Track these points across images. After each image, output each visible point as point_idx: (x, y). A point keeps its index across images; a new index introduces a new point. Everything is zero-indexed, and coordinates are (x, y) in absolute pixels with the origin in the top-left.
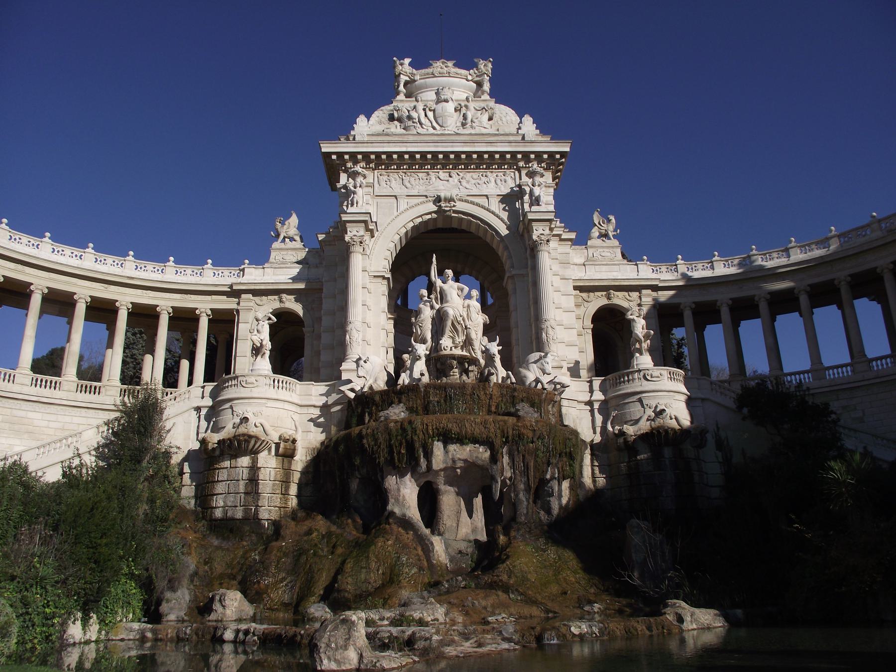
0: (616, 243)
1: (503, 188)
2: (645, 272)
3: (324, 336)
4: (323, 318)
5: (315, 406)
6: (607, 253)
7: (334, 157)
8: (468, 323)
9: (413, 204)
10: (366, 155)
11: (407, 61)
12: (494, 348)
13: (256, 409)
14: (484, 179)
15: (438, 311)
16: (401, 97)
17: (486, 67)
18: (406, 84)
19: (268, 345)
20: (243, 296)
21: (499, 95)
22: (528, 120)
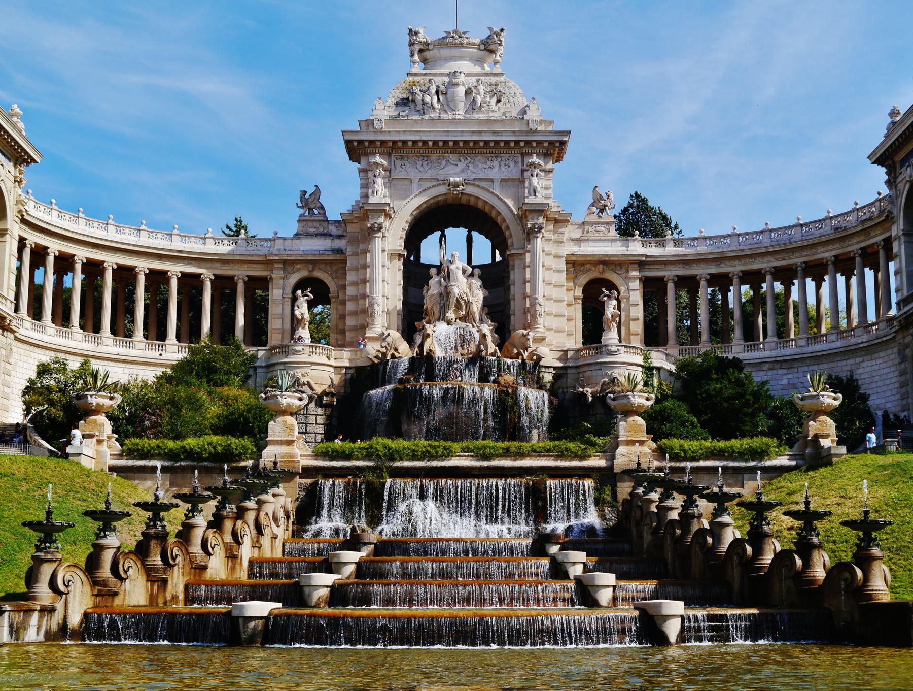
1: (506, 173)
3: (348, 303)
4: (348, 288)
7: (355, 144)
8: (471, 298)
9: (426, 187)
10: (383, 142)
12: (487, 329)
13: (304, 371)
14: (489, 163)
15: (446, 287)
18: (421, 51)
19: (307, 316)
20: (276, 265)
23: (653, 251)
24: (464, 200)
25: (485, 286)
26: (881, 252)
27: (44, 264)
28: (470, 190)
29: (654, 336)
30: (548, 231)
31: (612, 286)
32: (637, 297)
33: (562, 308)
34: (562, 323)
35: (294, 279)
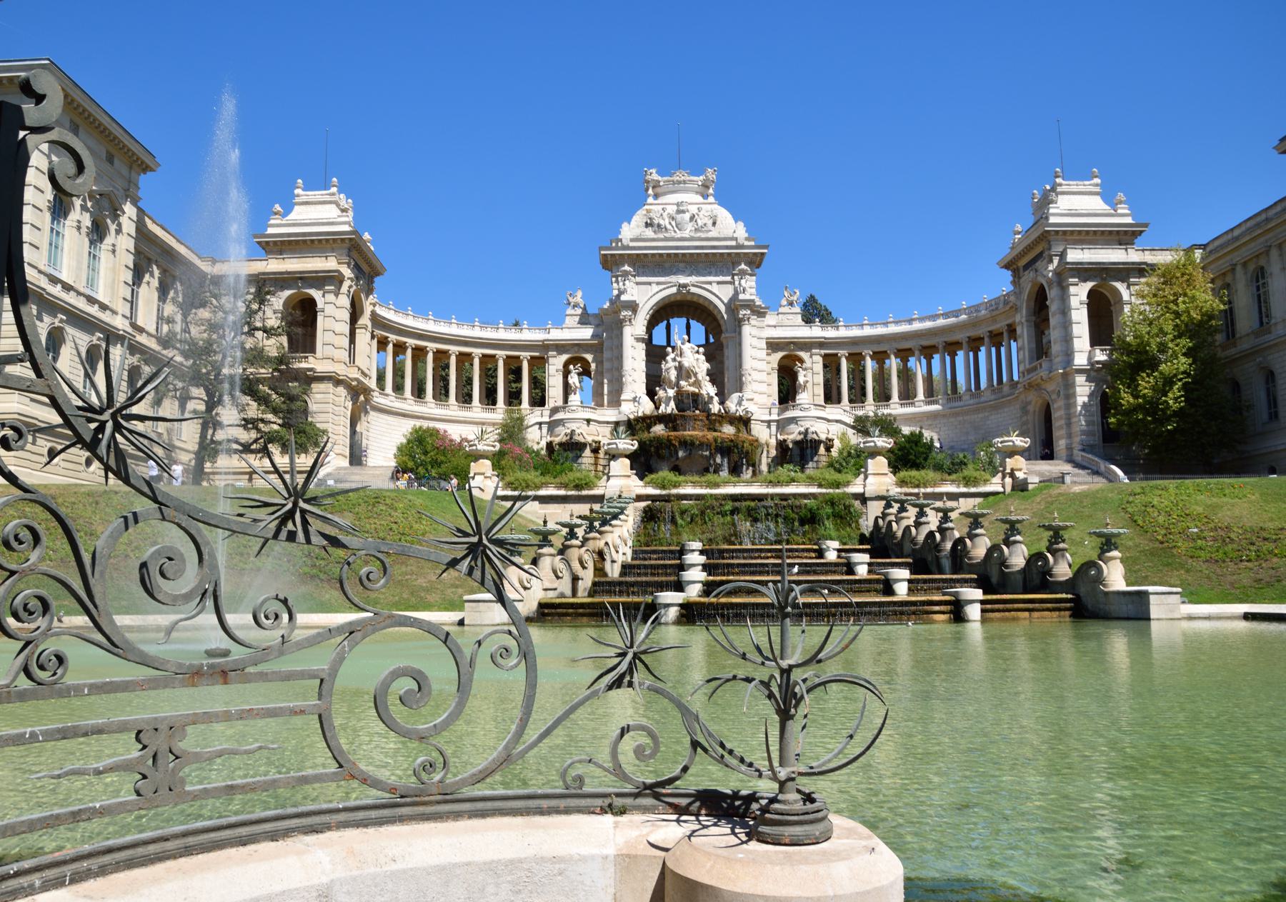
0: (797, 309)
2: (816, 331)
5: (608, 423)
6: (790, 317)
11: (654, 171)
16: (650, 200)
17: (711, 174)
21: (722, 202)
22: (741, 225)
23: (830, 333)
24: (689, 298)
25: (708, 361)
26: (1005, 335)
27: (385, 350)
28: (693, 290)
29: (831, 396)
30: (754, 320)
31: (802, 361)
32: (819, 367)
33: (763, 376)
34: (763, 388)
35: (565, 357)
